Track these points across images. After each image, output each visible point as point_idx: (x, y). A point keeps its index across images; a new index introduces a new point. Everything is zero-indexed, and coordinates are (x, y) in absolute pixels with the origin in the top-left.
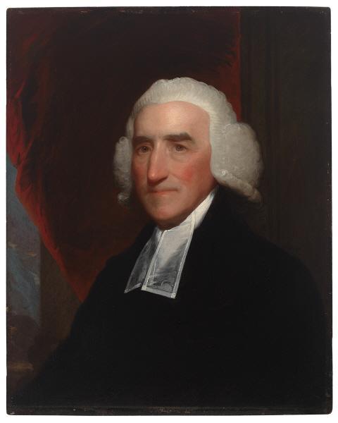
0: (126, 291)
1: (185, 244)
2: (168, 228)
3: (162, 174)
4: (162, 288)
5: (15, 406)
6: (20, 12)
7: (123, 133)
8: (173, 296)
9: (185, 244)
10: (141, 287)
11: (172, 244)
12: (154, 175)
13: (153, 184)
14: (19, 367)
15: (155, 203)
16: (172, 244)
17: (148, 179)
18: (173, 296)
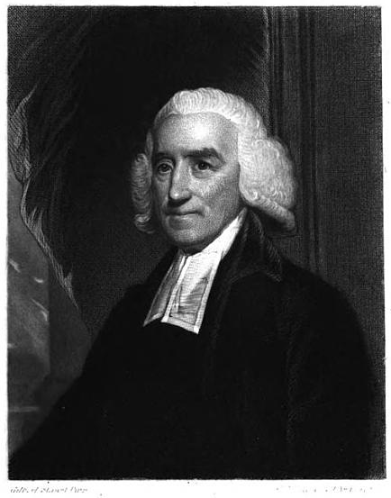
0: (146, 323)
1: (210, 271)
2: (192, 254)
3: (186, 193)
4: (184, 319)
5: (20, 468)
6: (379, 86)
7: (141, 149)
8: (196, 330)
9: (210, 271)
10: (161, 318)
11: (198, 270)
12: (176, 195)
13: (175, 204)
14: (17, 409)
15: (178, 226)
16: (198, 270)
17: (170, 198)
18: (196, 330)
